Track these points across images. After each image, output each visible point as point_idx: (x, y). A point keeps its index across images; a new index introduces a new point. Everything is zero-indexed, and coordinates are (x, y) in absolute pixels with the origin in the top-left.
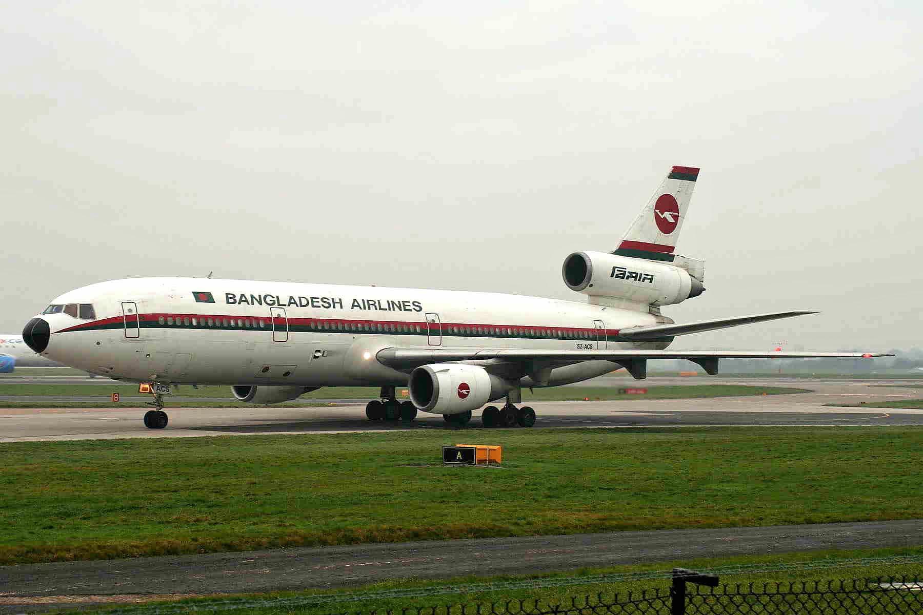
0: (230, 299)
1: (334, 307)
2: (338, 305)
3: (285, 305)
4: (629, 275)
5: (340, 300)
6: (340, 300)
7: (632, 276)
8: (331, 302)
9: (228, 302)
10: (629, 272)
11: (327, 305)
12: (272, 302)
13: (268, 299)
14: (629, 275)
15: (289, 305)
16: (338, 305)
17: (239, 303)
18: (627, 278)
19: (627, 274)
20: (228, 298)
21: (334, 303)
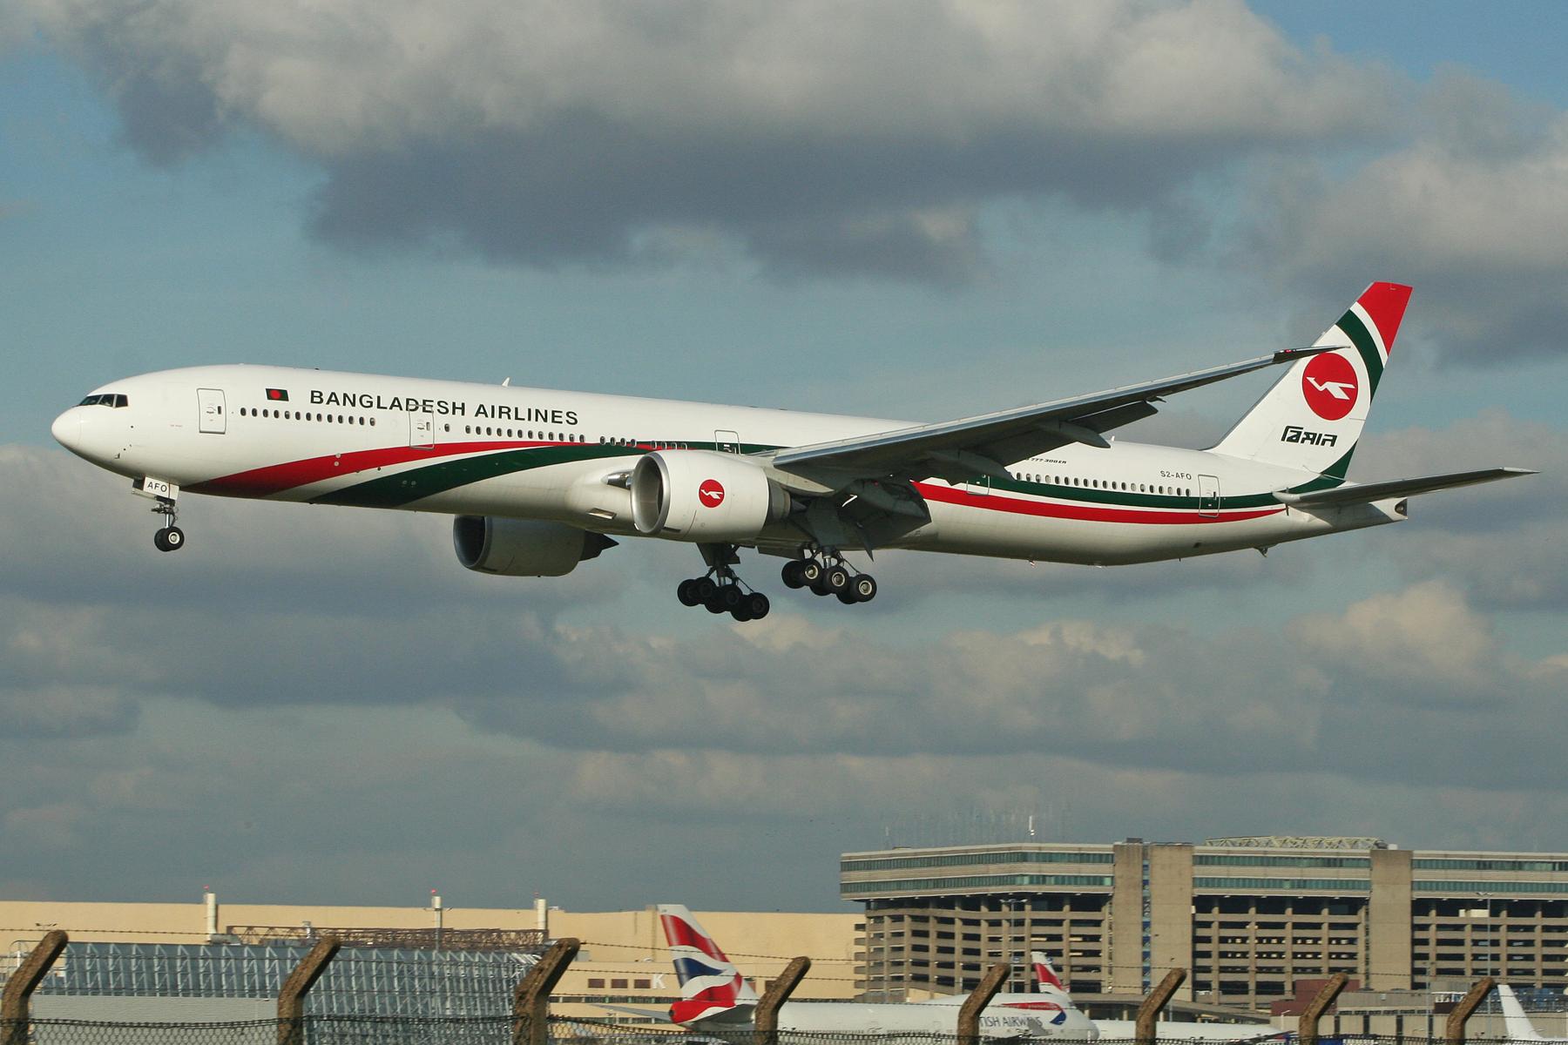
0: (316, 397)
1: (454, 413)
2: (458, 412)
3: (386, 408)
4: (1305, 436)
5: (463, 404)
6: (463, 404)
7: (1308, 438)
8: (450, 407)
9: (312, 401)
10: (1305, 433)
11: (444, 410)
12: (369, 404)
13: (365, 400)
14: (1305, 436)
15: (391, 408)
16: (458, 412)
17: (328, 403)
18: (1302, 442)
19: (1303, 436)
20: (313, 397)
21: (454, 408)
